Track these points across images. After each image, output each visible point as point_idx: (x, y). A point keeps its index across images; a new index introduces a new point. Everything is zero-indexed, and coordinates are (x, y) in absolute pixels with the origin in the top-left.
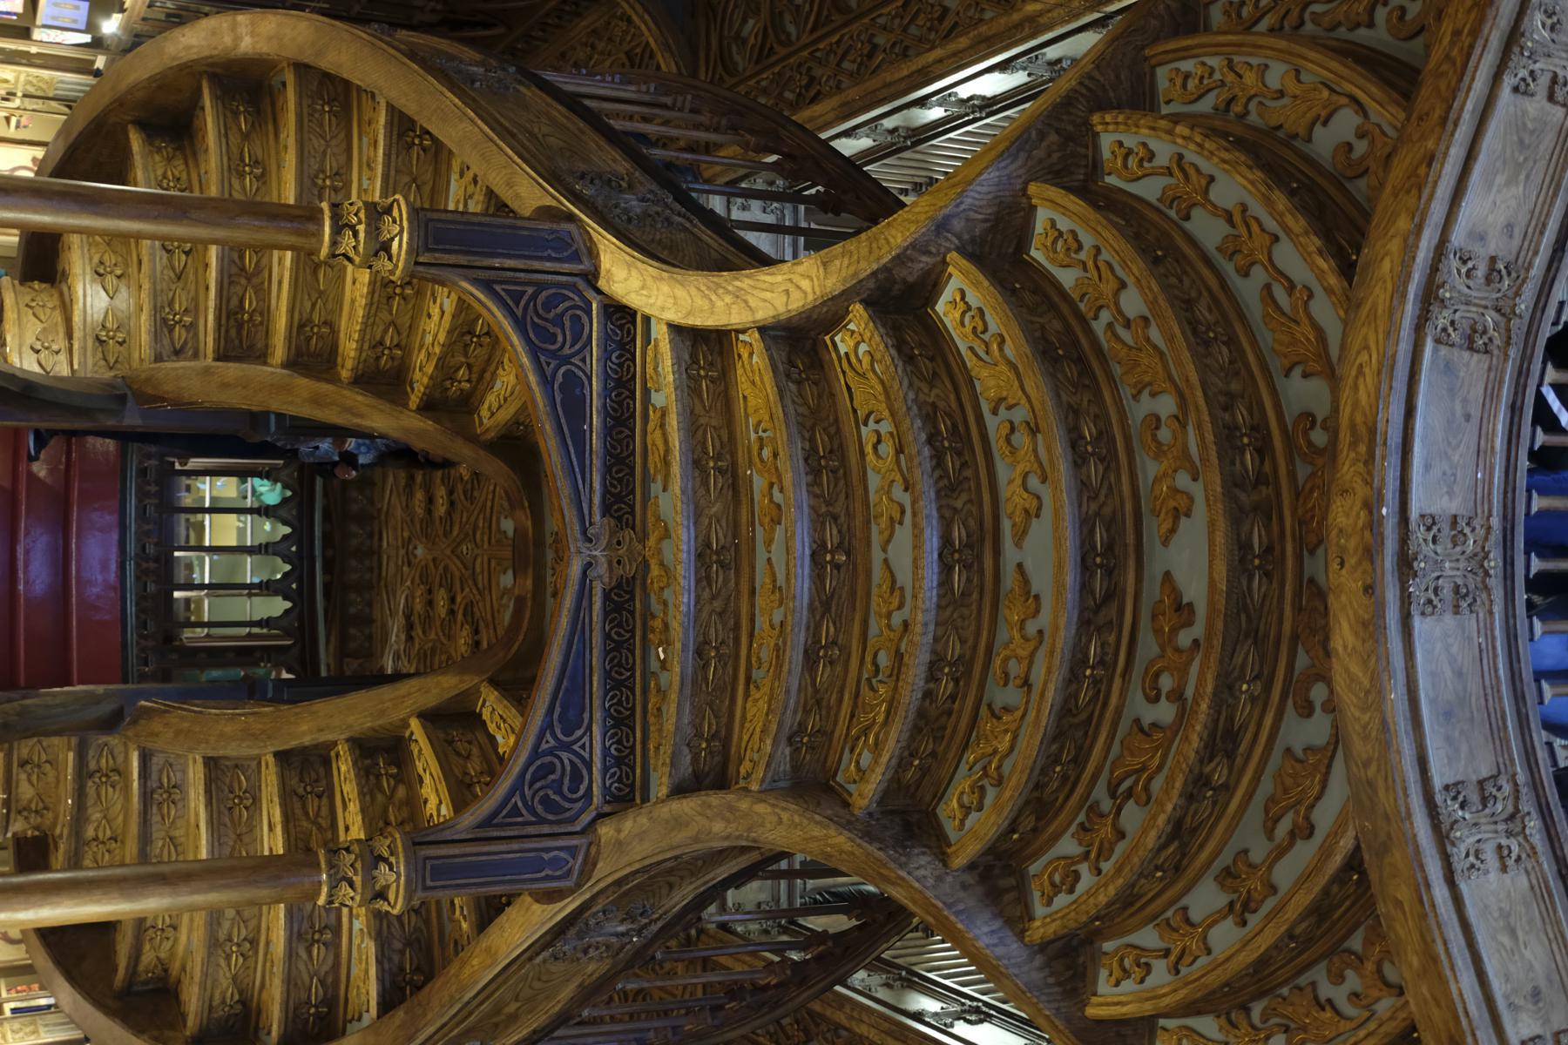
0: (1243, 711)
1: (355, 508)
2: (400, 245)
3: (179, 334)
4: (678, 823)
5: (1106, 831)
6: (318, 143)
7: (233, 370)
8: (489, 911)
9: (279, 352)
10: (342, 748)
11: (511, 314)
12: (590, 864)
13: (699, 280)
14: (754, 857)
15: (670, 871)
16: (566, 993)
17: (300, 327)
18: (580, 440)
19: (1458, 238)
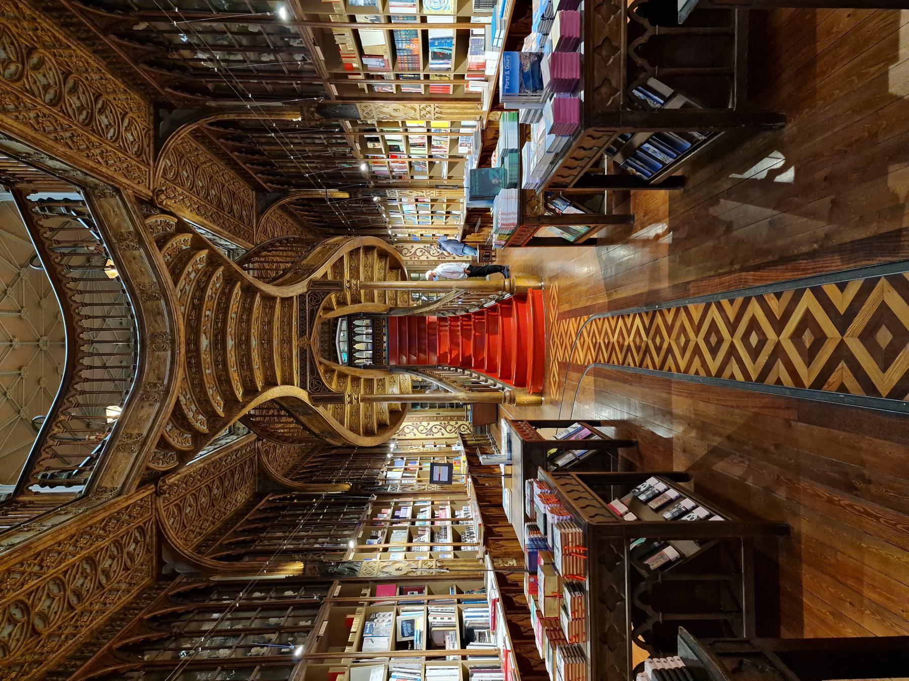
0: (193, 313)
1: (327, 353)
2: (347, 396)
3: (380, 384)
4: (292, 292)
5: (214, 289)
6: (356, 421)
7: (370, 377)
8: (325, 275)
9: (362, 380)
10: (349, 303)
11: (325, 386)
12: (309, 284)
13: (290, 394)
14: (274, 283)
15: (292, 281)
16: (309, 257)
17: (358, 386)
18: (311, 363)
19: (158, 405)
